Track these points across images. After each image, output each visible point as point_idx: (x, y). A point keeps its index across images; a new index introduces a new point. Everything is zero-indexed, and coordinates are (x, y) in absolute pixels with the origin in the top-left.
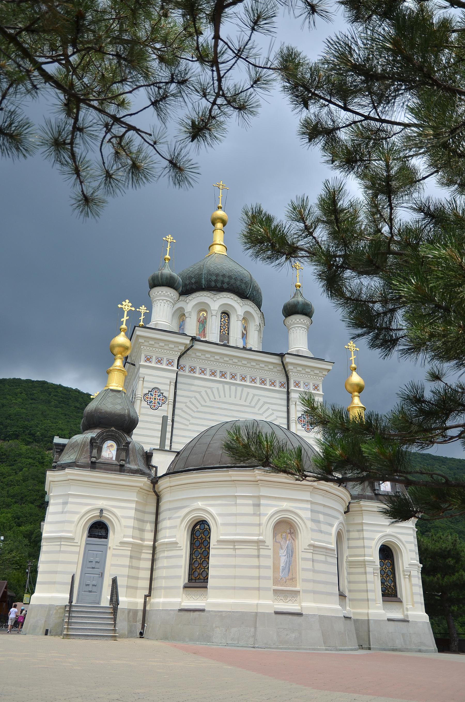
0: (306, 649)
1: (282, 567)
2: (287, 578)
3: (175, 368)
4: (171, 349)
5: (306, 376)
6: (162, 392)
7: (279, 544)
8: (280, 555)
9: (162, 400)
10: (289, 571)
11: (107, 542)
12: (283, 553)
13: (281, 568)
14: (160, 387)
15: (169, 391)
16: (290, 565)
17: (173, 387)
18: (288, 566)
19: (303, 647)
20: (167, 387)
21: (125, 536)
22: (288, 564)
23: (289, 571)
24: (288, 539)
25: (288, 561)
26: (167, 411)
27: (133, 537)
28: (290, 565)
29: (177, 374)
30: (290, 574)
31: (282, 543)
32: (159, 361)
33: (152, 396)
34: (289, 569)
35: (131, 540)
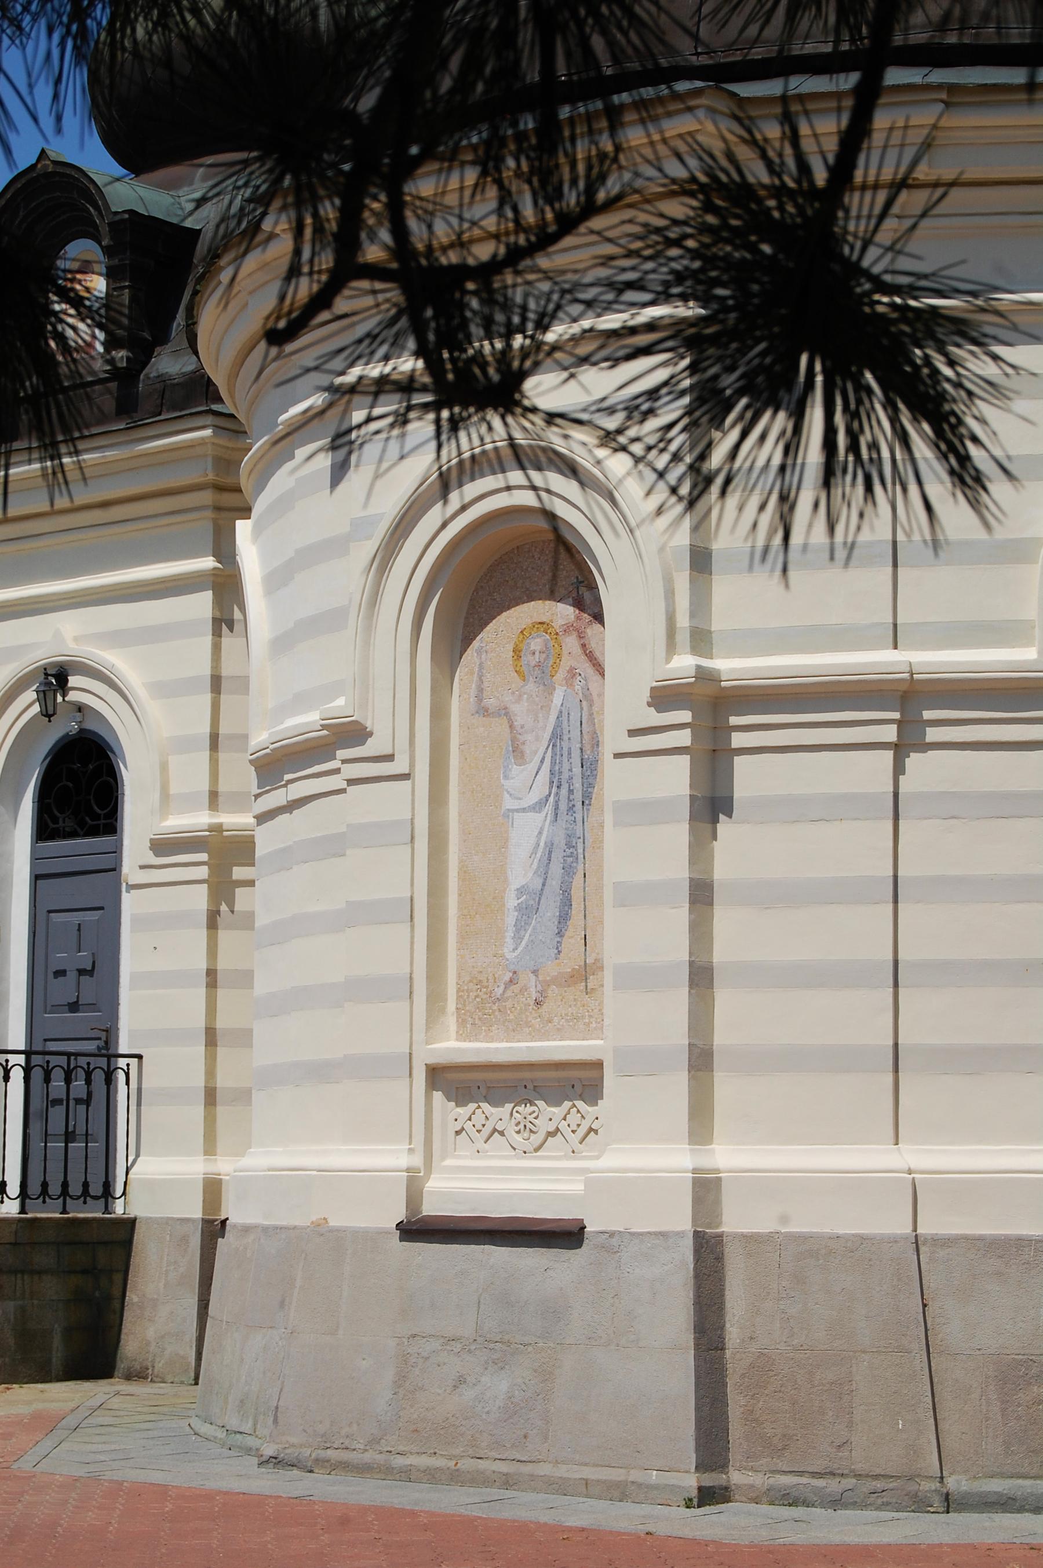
0: (562, 1487)
1: (521, 891)
2: (551, 969)
7: (500, 727)
8: (509, 803)
10: (564, 918)
11: (117, 851)
12: (526, 783)
13: (512, 902)
16: (569, 871)
18: (554, 883)
19: (544, 1469)
22: (556, 869)
23: (564, 918)
24: (561, 675)
25: (560, 840)
28: (569, 871)
30: (572, 941)
31: (520, 712)
34: (567, 902)
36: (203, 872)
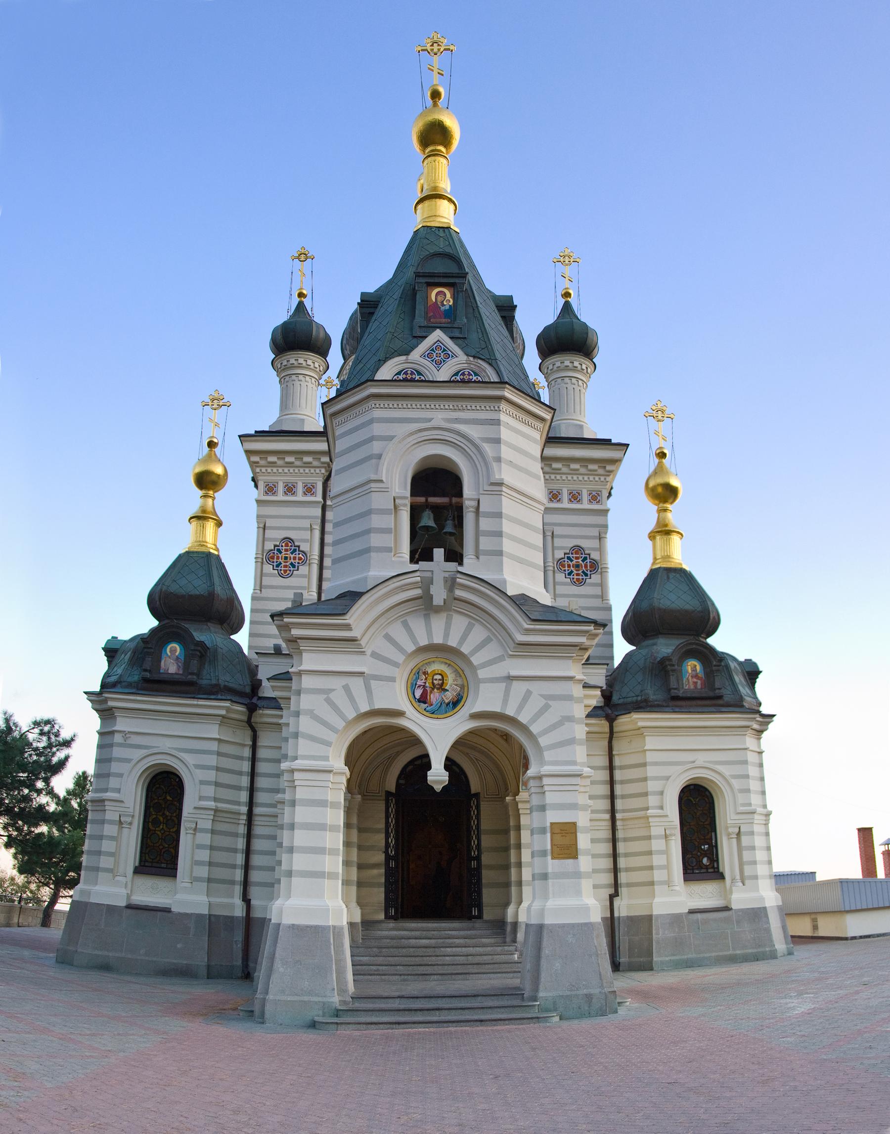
3: (319, 498)
4: (308, 465)
5: (570, 478)
6: (296, 544)
9: (300, 559)
14: (292, 535)
15: (311, 541)
17: (317, 534)
20: (307, 535)
21: (201, 798)
26: (309, 577)
27: (216, 800)
29: (324, 508)
32: (290, 489)
33: (281, 553)
35: (212, 804)
36: (212, 817)
